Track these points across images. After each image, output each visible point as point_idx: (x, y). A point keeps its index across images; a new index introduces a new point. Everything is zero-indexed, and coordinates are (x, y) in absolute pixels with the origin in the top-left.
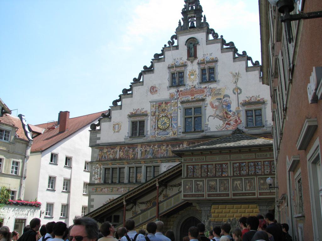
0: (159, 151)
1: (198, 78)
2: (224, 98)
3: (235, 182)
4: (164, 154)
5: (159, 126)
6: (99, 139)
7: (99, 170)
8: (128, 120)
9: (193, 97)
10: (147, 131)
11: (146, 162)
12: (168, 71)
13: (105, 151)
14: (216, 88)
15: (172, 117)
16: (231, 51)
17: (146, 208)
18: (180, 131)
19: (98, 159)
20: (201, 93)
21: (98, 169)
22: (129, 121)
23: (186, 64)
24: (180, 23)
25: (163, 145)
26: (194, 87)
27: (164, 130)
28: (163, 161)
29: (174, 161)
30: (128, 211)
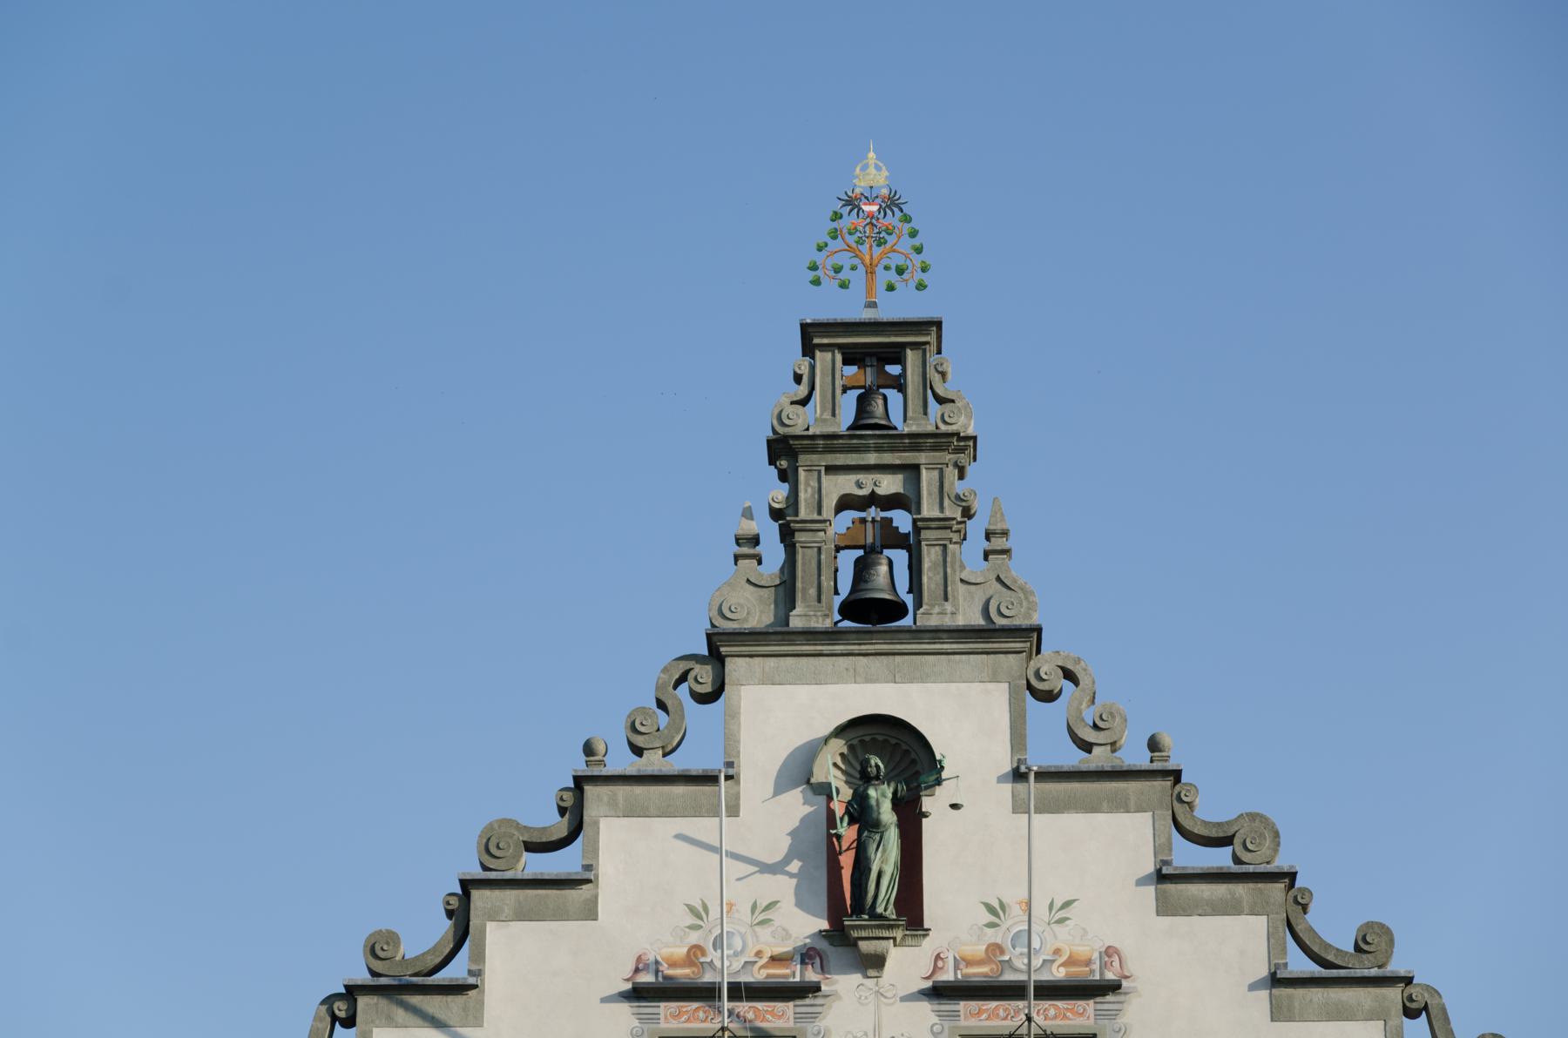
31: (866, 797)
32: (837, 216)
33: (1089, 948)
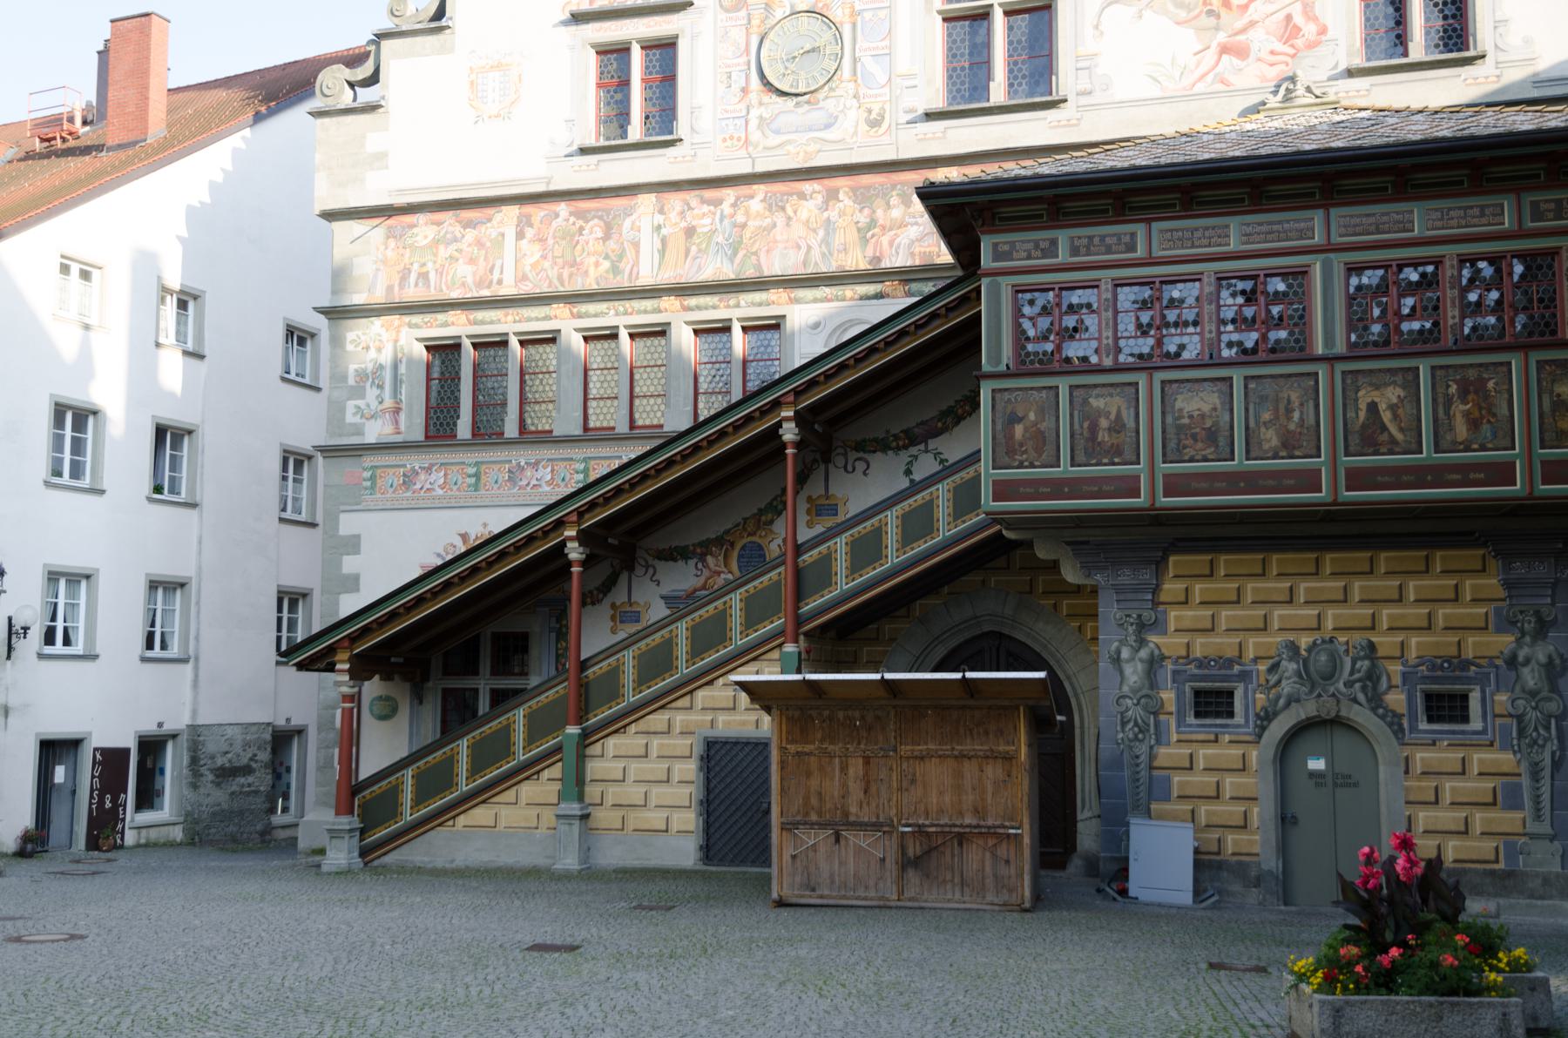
0: (779, 233)
3: (1365, 397)
4: (809, 247)
6: (380, 158)
17: (700, 582)
25: (802, 196)
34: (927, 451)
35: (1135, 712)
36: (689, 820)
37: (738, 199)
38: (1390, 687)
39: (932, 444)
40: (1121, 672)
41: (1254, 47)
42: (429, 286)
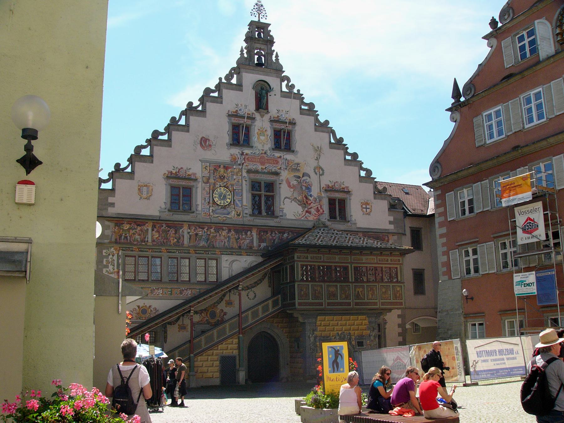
0: (218, 238)
1: (270, 140)
2: (303, 177)
3: (357, 289)
5: (216, 200)
6: (113, 205)
7: (115, 258)
8: (165, 183)
9: (264, 167)
10: (197, 205)
11: (198, 252)
12: (226, 119)
13: (126, 227)
14: (293, 161)
15: (234, 190)
16: (312, 116)
17: (201, 319)
18: (246, 211)
19: (113, 240)
20: (274, 163)
21: (113, 256)
22: (166, 185)
23: (254, 116)
24: (242, 51)
25: (223, 230)
26: (265, 153)
27: (224, 207)
28: (223, 253)
29: (239, 253)
30: (171, 325)
31: (262, 92)
32: (254, 6)
33: (291, 118)
34: (251, 291)
35: (313, 347)
36: (217, 374)
37: (208, 228)
38: (353, 340)
39: (253, 289)
40: (310, 339)
41: (312, 212)
42: (128, 240)
